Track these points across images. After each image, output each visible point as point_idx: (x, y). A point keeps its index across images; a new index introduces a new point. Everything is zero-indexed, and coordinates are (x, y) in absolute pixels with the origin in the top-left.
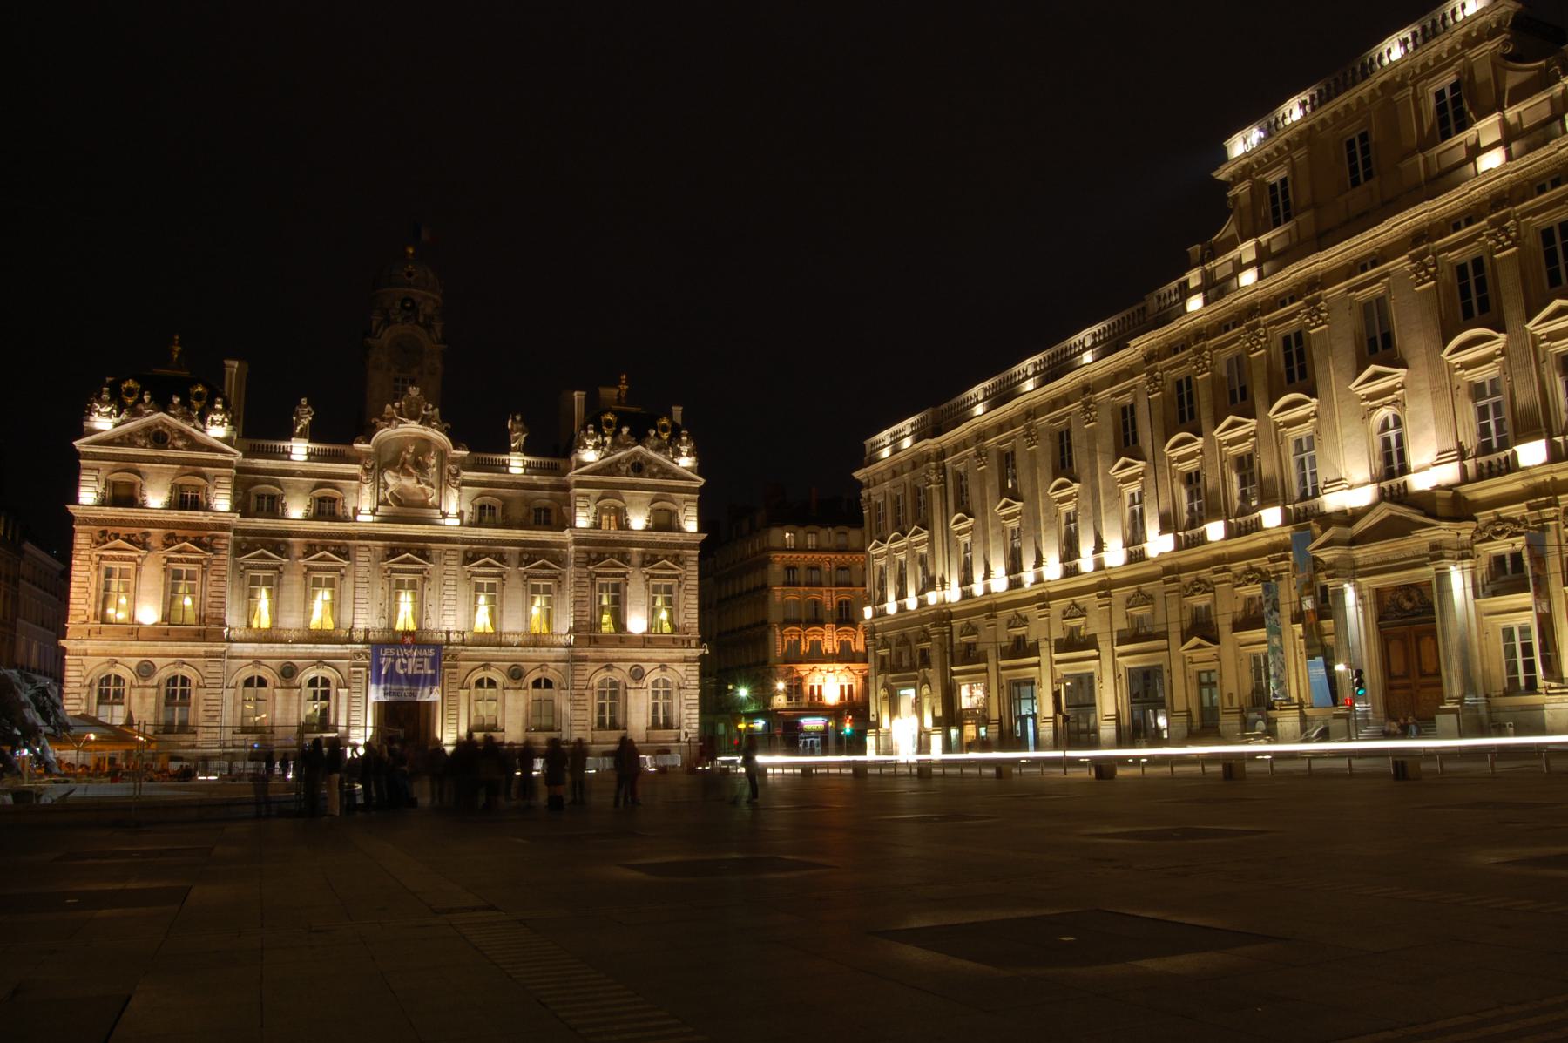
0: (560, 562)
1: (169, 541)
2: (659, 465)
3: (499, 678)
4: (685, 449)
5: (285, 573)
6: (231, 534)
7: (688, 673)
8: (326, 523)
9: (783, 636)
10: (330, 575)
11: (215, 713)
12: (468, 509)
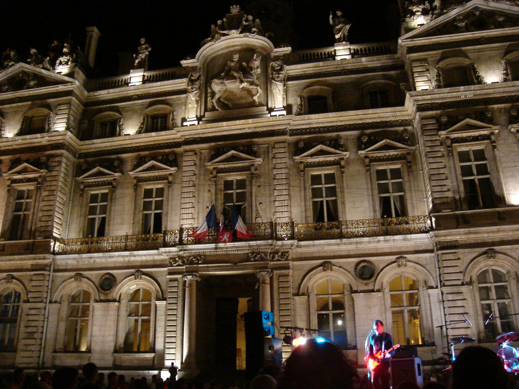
0: (407, 141)
5: (119, 187)
8: (153, 134)
11: (34, 329)
12: (295, 101)
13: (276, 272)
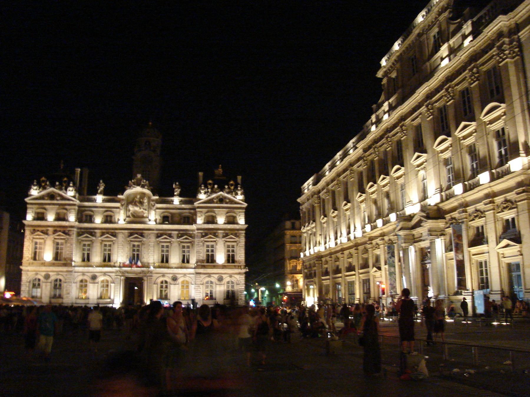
1: (55, 232)
2: (229, 199)
3: (169, 280)
4: (239, 193)
6: (75, 229)
7: (240, 278)
9: (290, 263)
10: (110, 243)
12: (158, 218)
13: (149, 278)
